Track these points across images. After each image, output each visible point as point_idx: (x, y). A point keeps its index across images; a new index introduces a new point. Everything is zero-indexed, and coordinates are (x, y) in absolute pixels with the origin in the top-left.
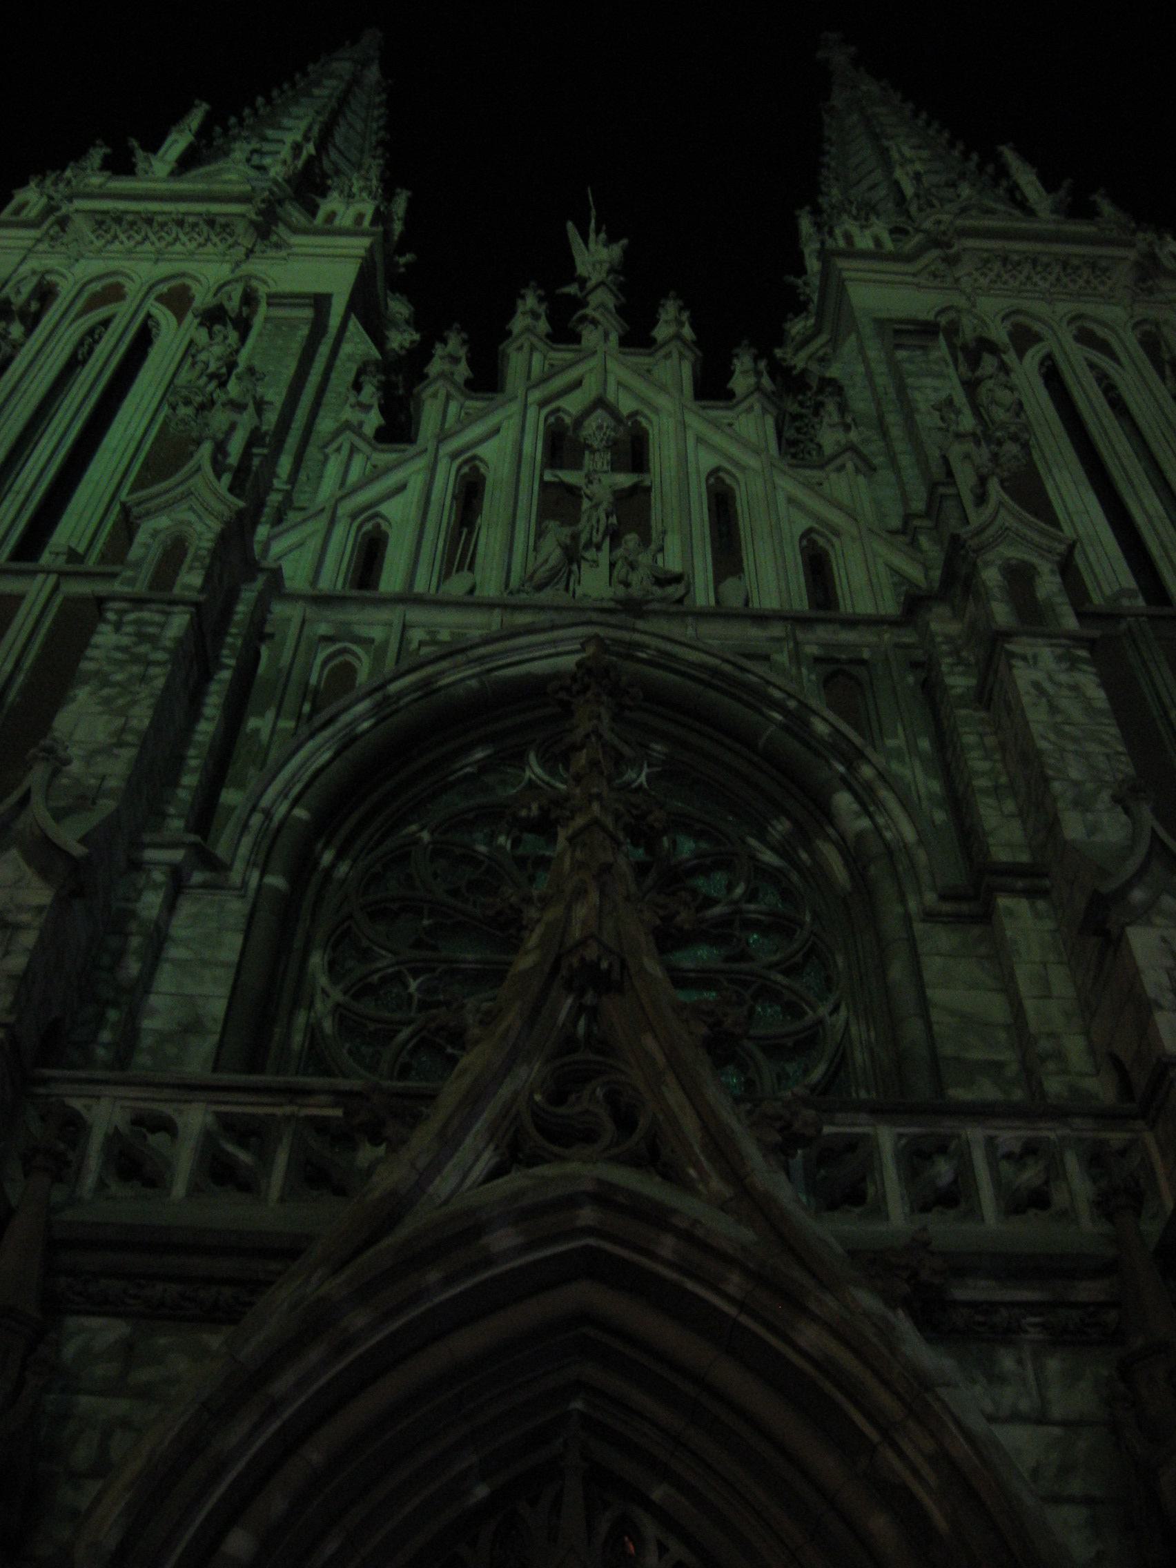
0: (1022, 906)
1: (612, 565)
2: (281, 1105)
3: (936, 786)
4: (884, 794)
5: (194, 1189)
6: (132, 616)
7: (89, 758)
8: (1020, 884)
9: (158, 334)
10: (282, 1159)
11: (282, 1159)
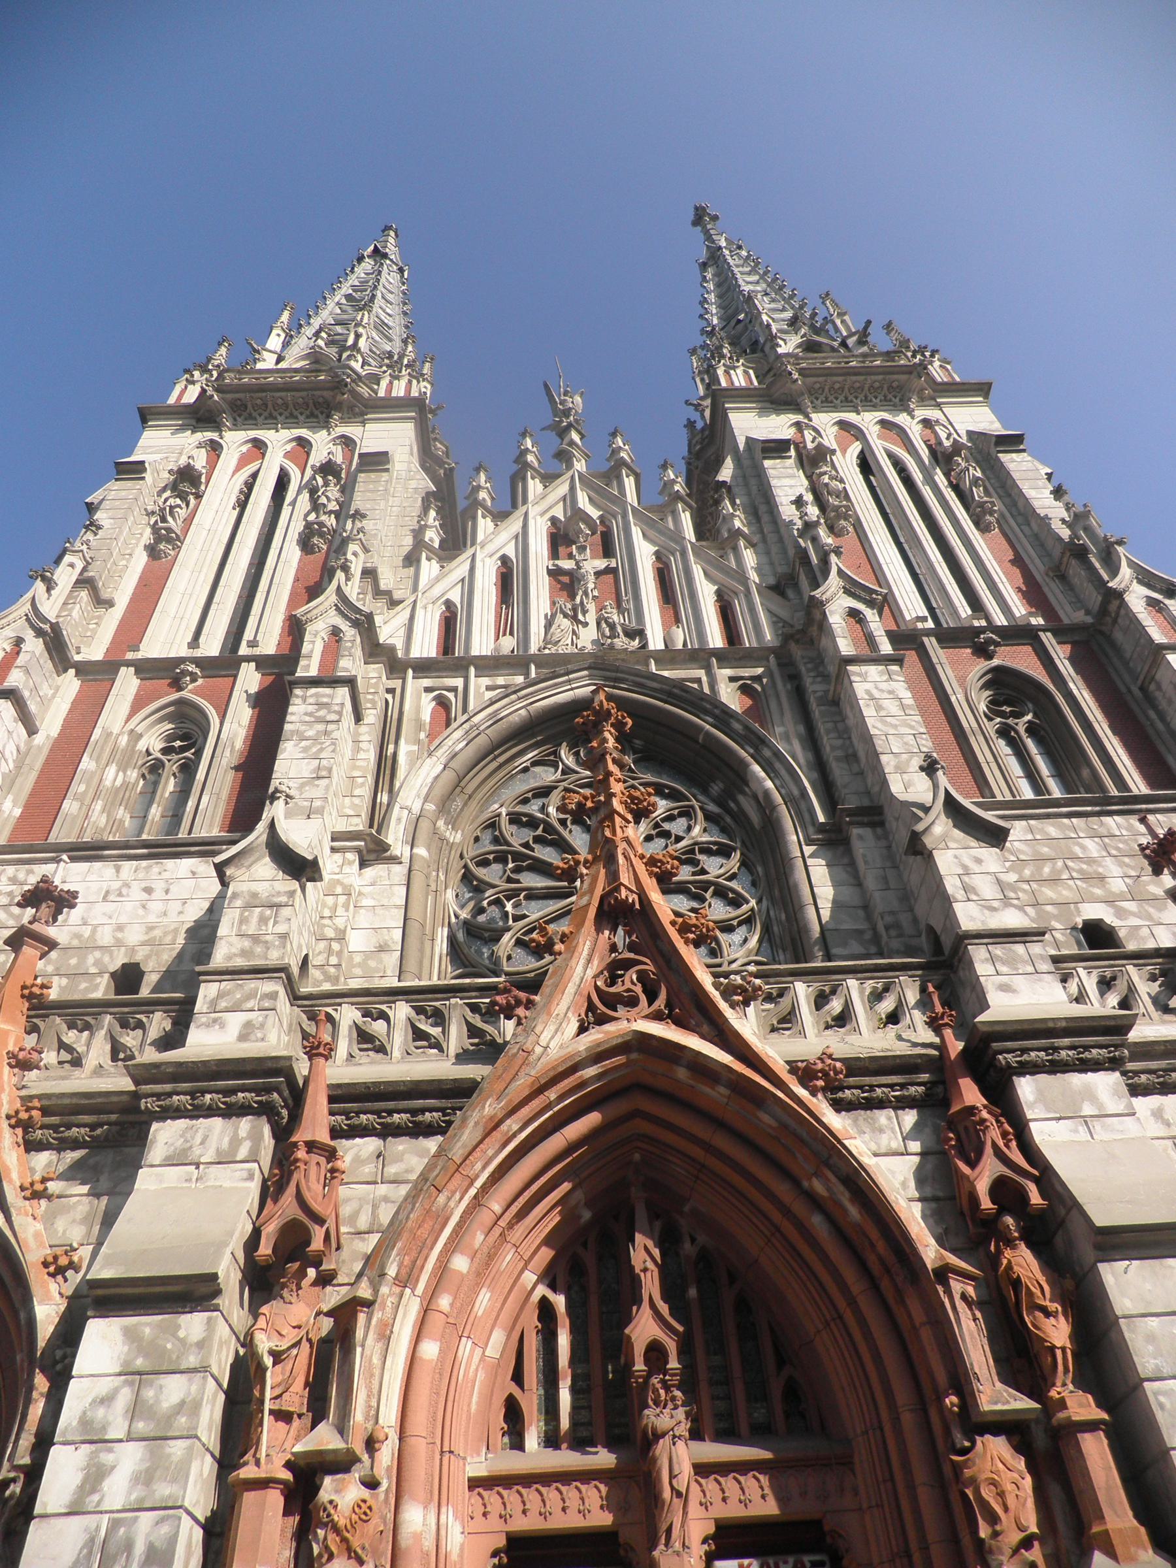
0: (866, 832)
1: (598, 624)
2: (448, 999)
6: (313, 691)
8: (866, 819)
10: (454, 1030)
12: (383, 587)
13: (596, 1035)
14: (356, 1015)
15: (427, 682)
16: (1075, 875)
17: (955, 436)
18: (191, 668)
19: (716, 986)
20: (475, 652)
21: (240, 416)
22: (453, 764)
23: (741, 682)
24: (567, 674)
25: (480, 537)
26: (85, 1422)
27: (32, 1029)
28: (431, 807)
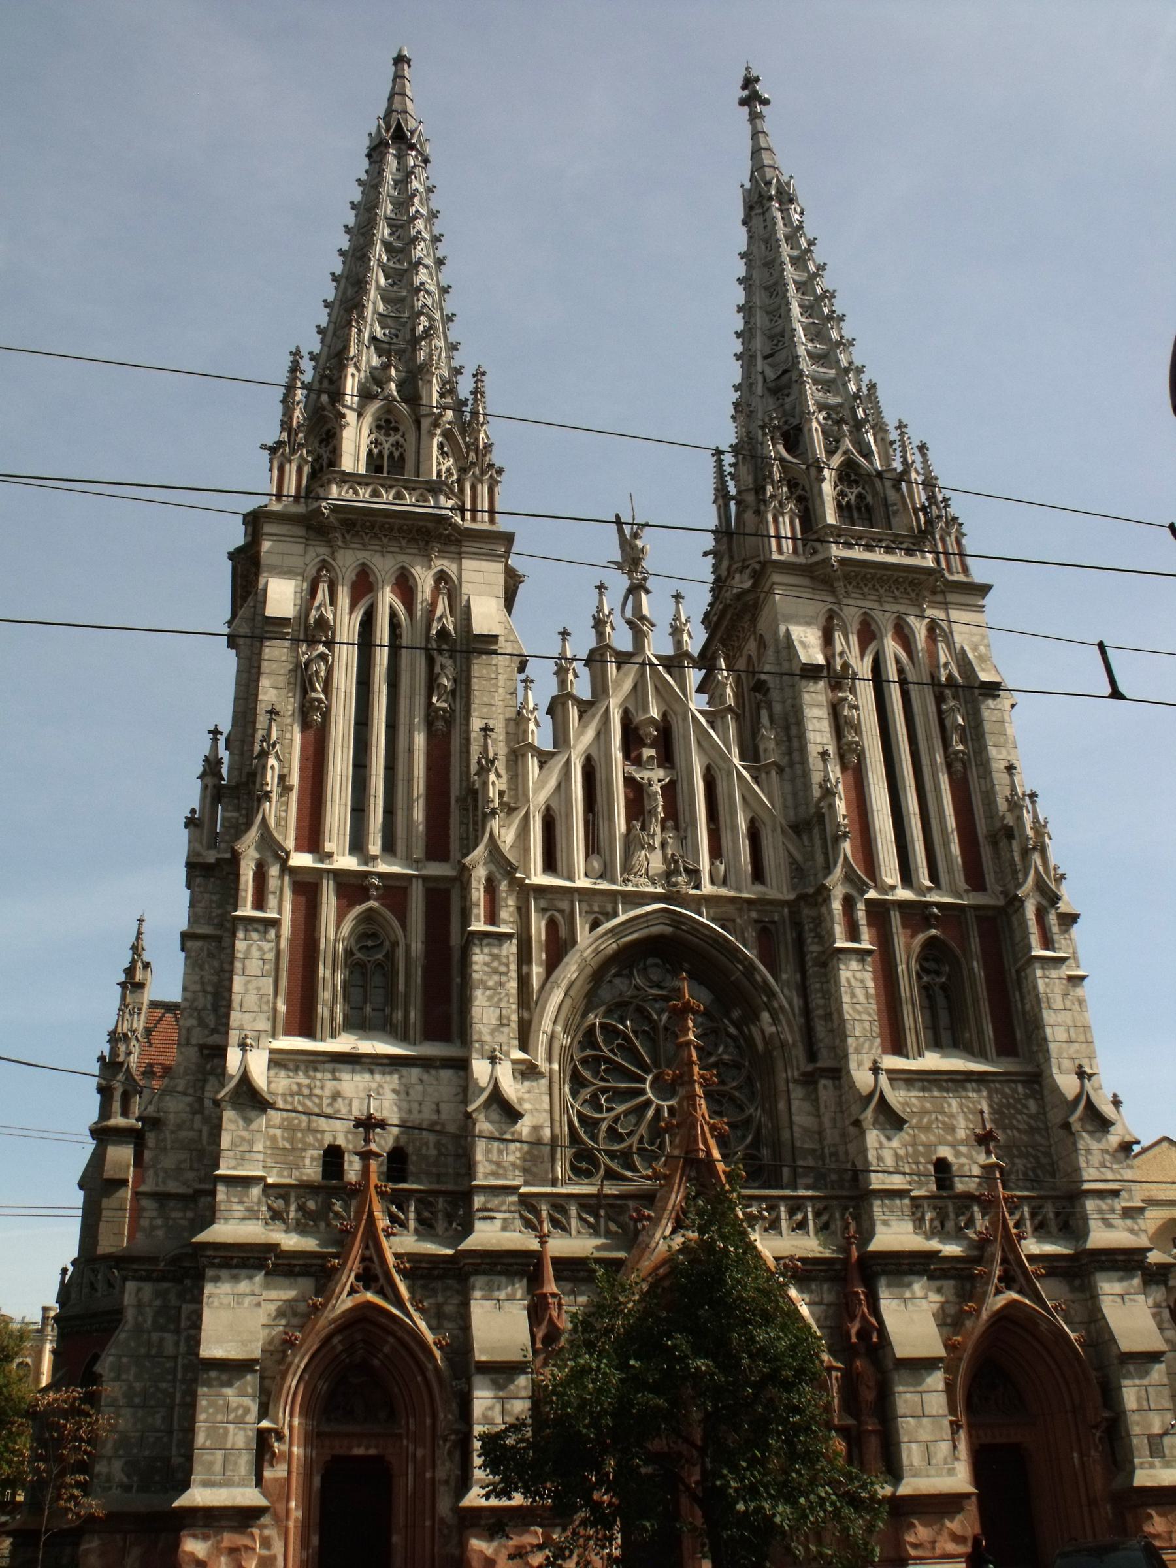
3: (801, 1002)
4: (781, 1017)
7: (492, 1033)
15: (543, 904)
21: (348, 532)
22: (572, 993)
23: (761, 925)
26: (484, 1416)
28: (559, 1029)
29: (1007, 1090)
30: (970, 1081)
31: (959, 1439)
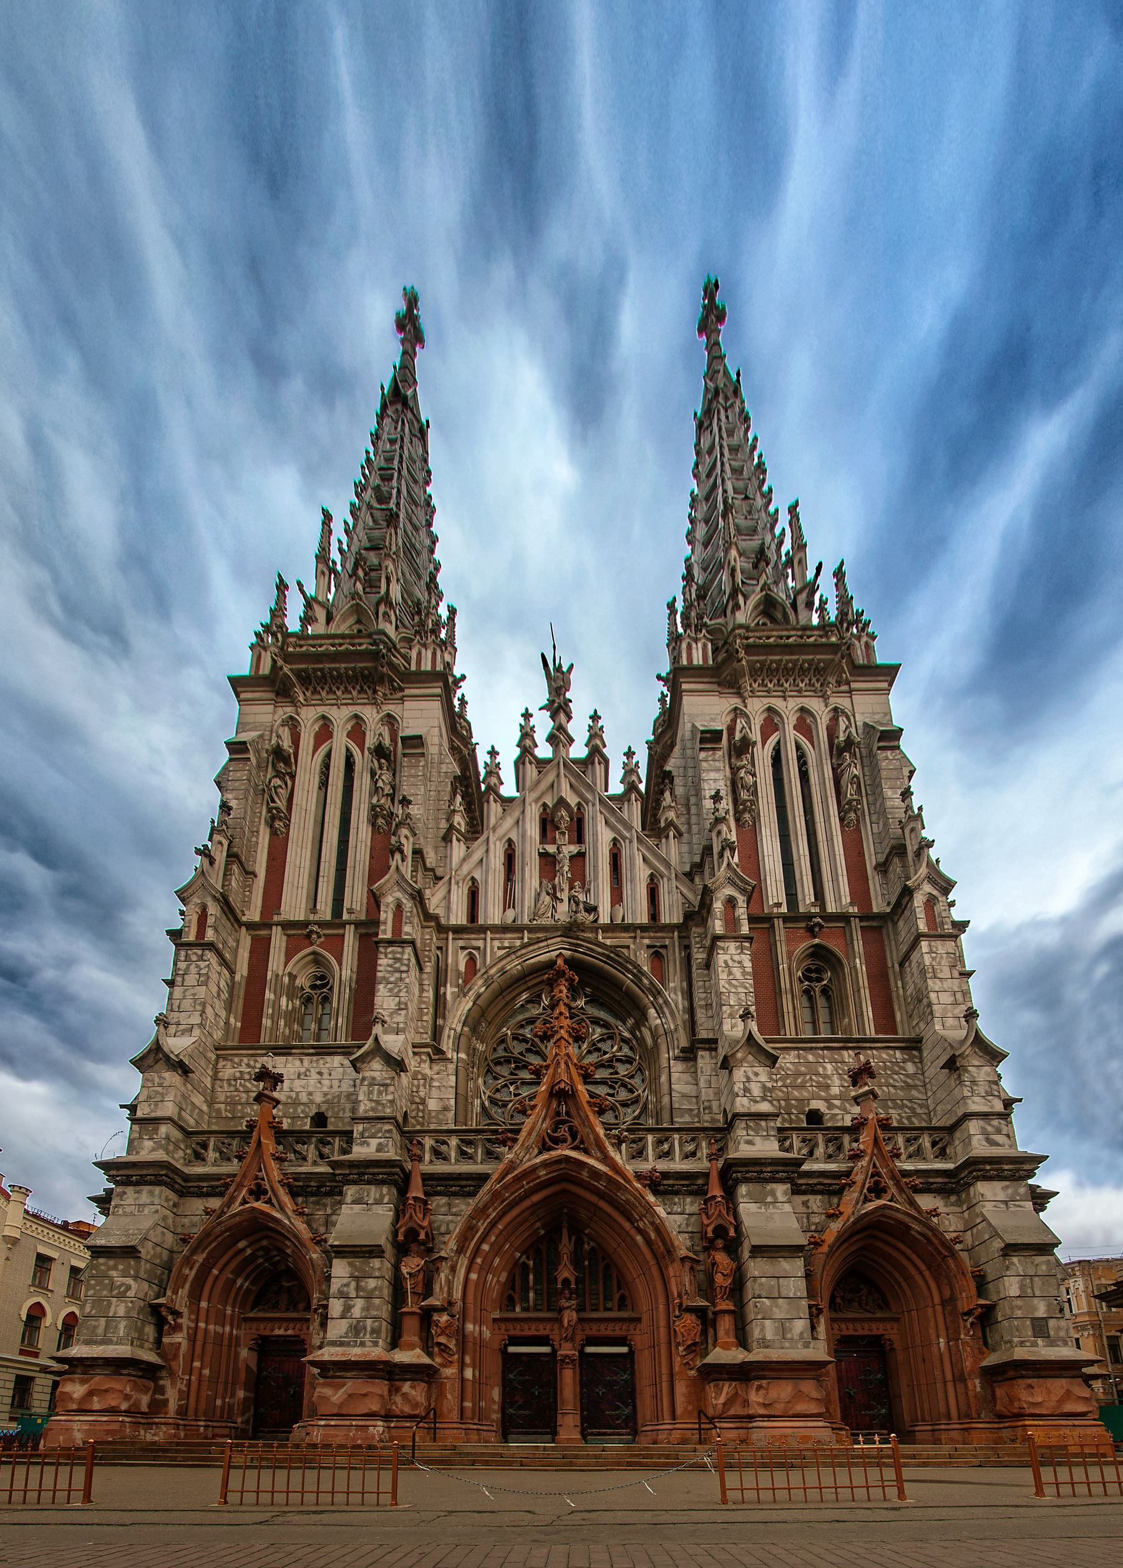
0: (706, 1054)
4: (666, 1010)
5: (457, 1161)
9: (354, 763)
10: (480, 1151)
11: (480, 1151)
12: (428, 865)
13: (545, 1156)
14: (432, 1142)
16: (814, 1084)
17: (853, 730)
18: (315, 928)
19: (606, 1135)
20: (490, 922)
24: (546, 940)
25: (493, 821)
27: (279, 1143)
29: (884, 1056)
30: (847, 1049)
31: (818, 1322)
